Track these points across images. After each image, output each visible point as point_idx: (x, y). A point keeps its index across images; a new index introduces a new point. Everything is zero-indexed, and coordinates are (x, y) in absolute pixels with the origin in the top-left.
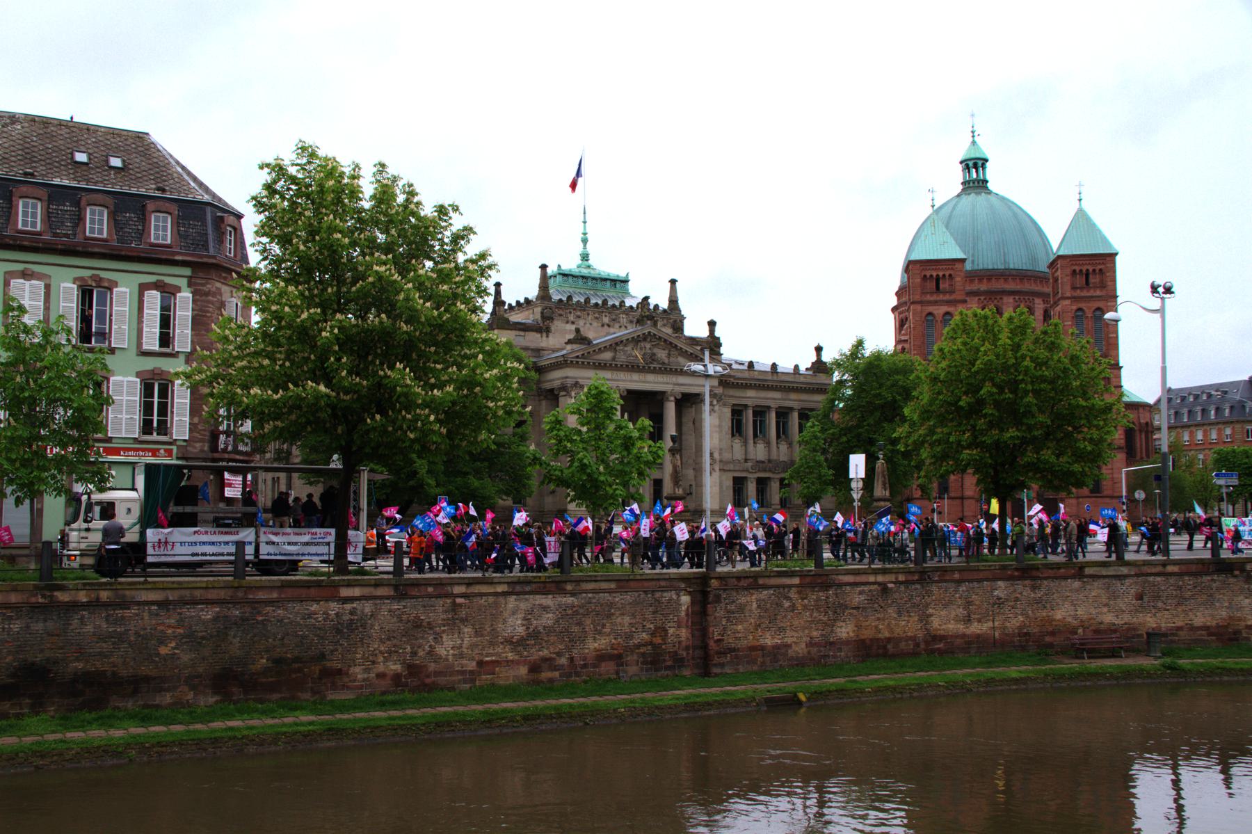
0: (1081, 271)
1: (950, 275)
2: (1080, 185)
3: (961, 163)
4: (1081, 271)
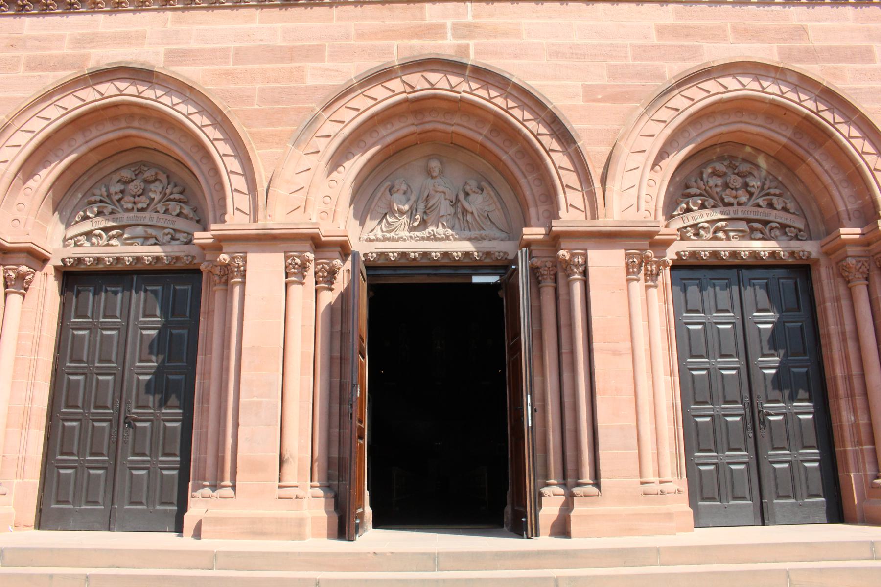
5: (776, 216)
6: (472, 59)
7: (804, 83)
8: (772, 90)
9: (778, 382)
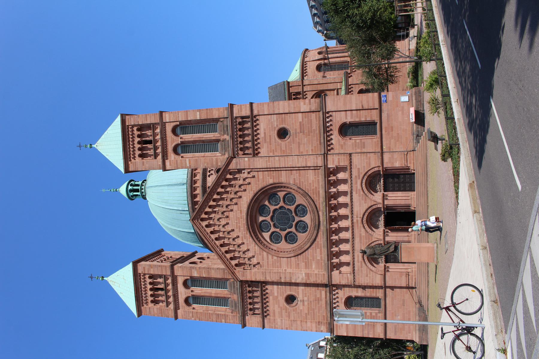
0: (140, 149)
1: (150, 277)
2: (80, 146)
3: (133, 200)
4: (140, 149)
5: (378, 178)
6: (362, 216)
7: (363, 178)
8: (364, 181)
9: (398, 179)
